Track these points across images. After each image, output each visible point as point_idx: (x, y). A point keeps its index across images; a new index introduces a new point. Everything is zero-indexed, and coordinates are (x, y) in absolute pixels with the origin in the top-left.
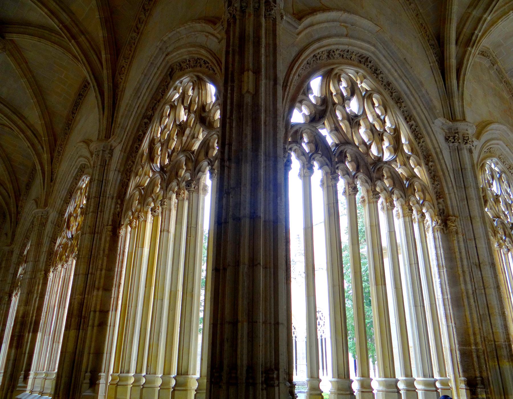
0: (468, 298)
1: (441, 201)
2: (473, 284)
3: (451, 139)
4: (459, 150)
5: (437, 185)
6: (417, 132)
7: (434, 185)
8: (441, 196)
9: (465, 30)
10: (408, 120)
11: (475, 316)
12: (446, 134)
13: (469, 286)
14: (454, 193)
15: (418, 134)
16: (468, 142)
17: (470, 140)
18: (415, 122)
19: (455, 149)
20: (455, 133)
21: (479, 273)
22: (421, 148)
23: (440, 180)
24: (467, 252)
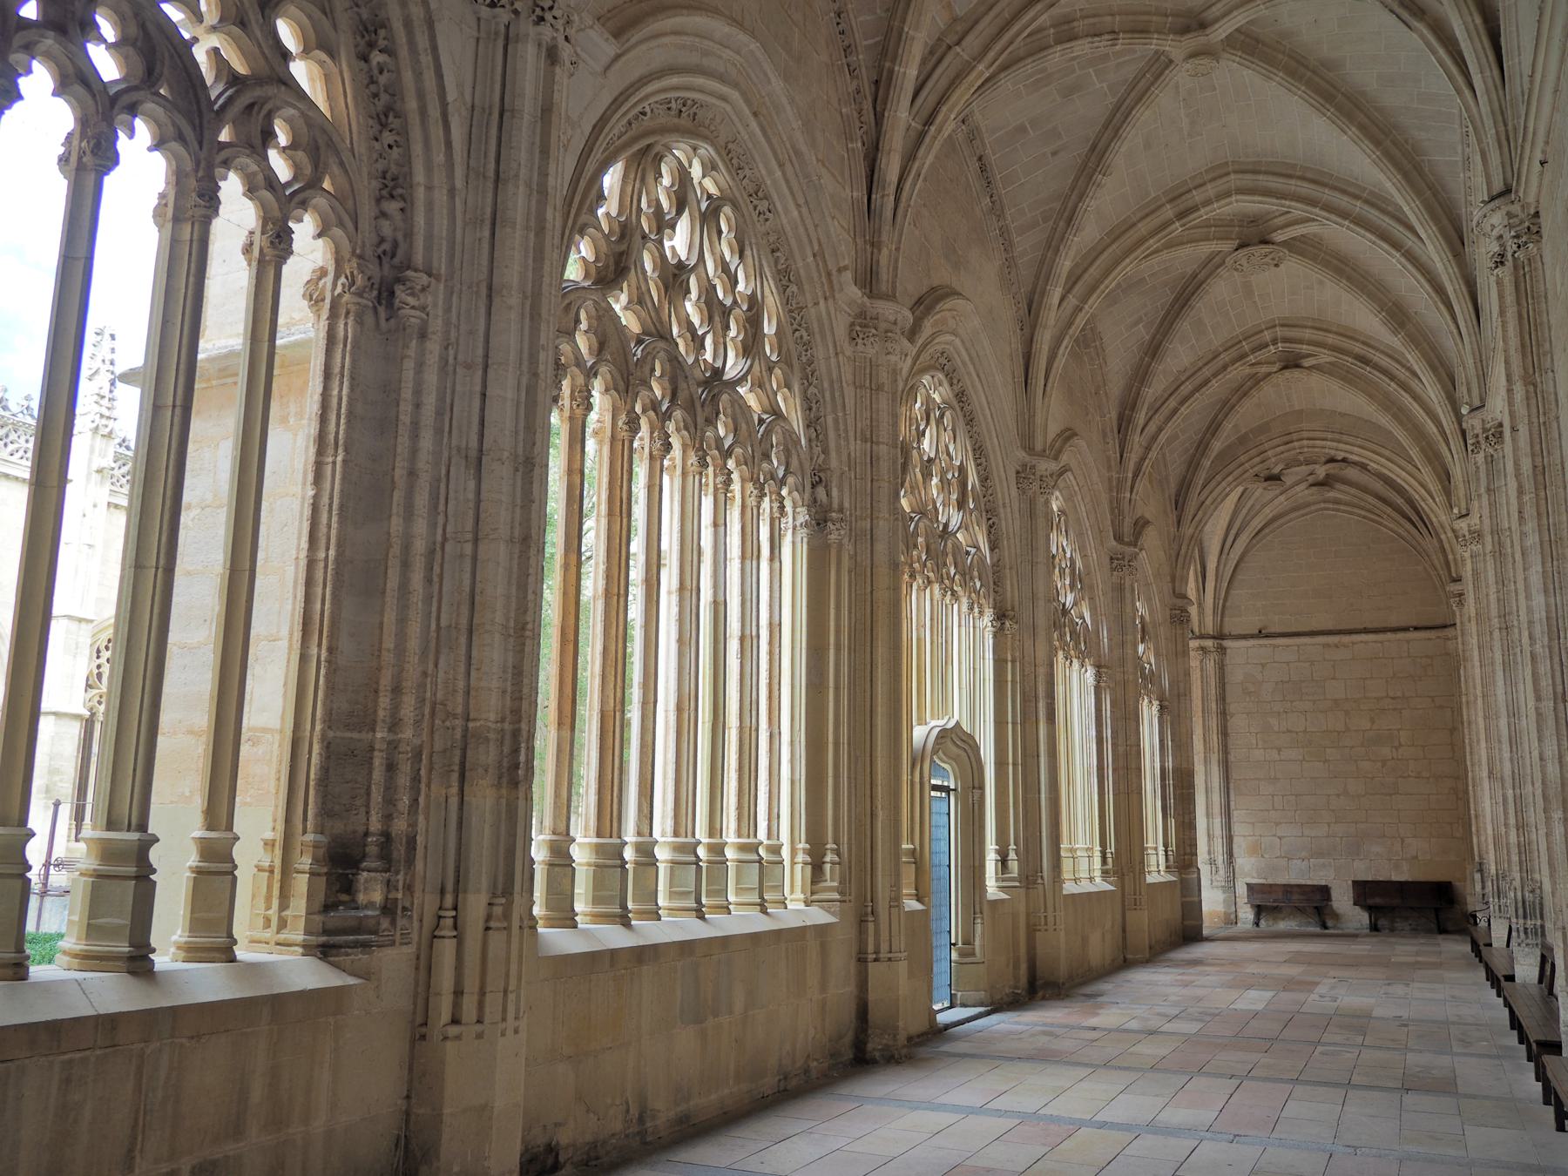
1: (392, 207)
5: (390, 147)
7: (377, 145)
8: (400, 191)
23: (404, 132)
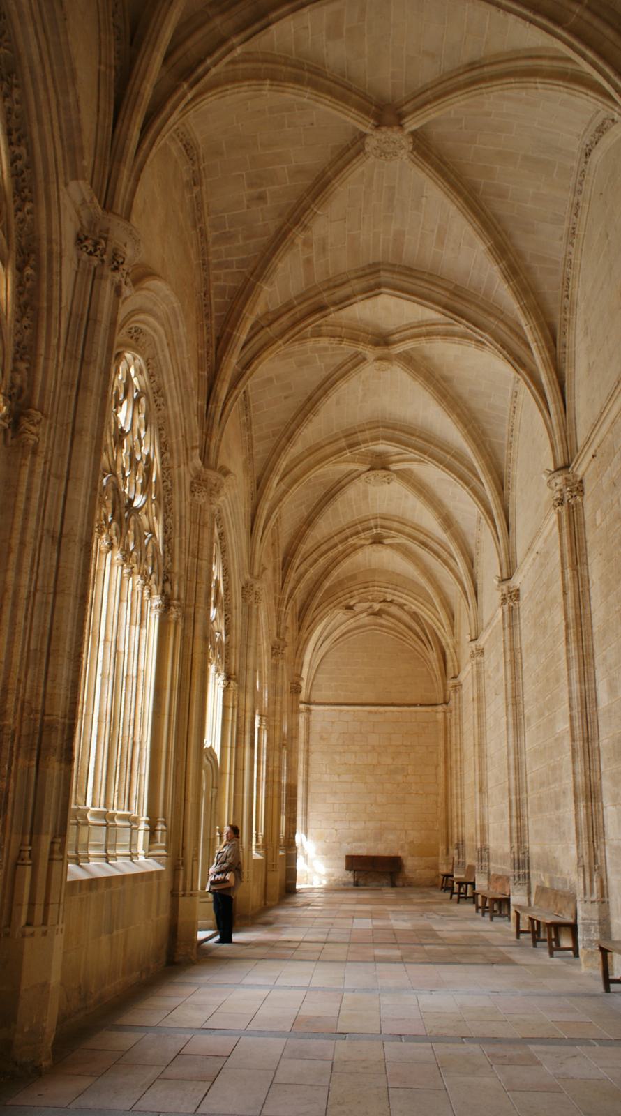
0: (15, 605)
2: (34, 577)
3: (89, 243)
4: (97, 276)
6: (23, 180)
7: (18, 325)
9: (189, 43)
10: (14, 138)
11: (17, 649)
12: (81, 230)
13: (25, 580)
14: (58, 361)
15: (25, 187)
16: (121, 268)
17: (125, 266)
18: (28, 154)
19: (89, 271)
20: (100, 237)
21: (55, 555)
22: (20, 225)
24: (42, 503)
